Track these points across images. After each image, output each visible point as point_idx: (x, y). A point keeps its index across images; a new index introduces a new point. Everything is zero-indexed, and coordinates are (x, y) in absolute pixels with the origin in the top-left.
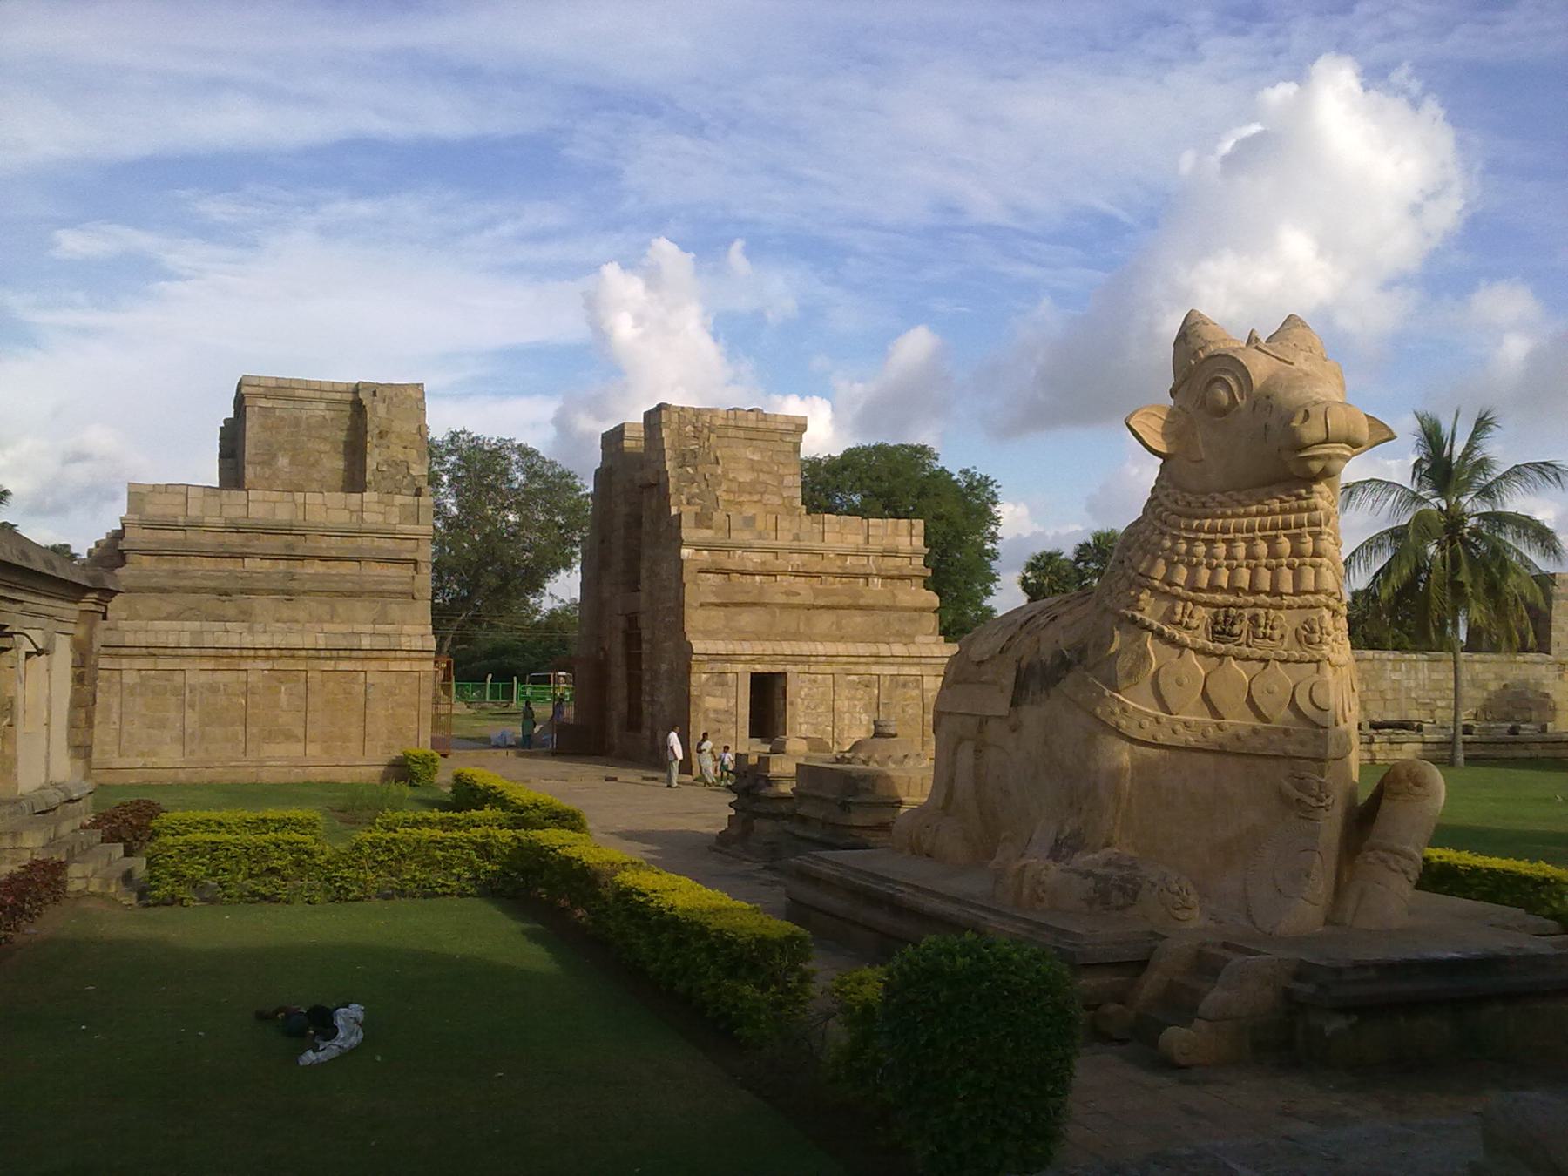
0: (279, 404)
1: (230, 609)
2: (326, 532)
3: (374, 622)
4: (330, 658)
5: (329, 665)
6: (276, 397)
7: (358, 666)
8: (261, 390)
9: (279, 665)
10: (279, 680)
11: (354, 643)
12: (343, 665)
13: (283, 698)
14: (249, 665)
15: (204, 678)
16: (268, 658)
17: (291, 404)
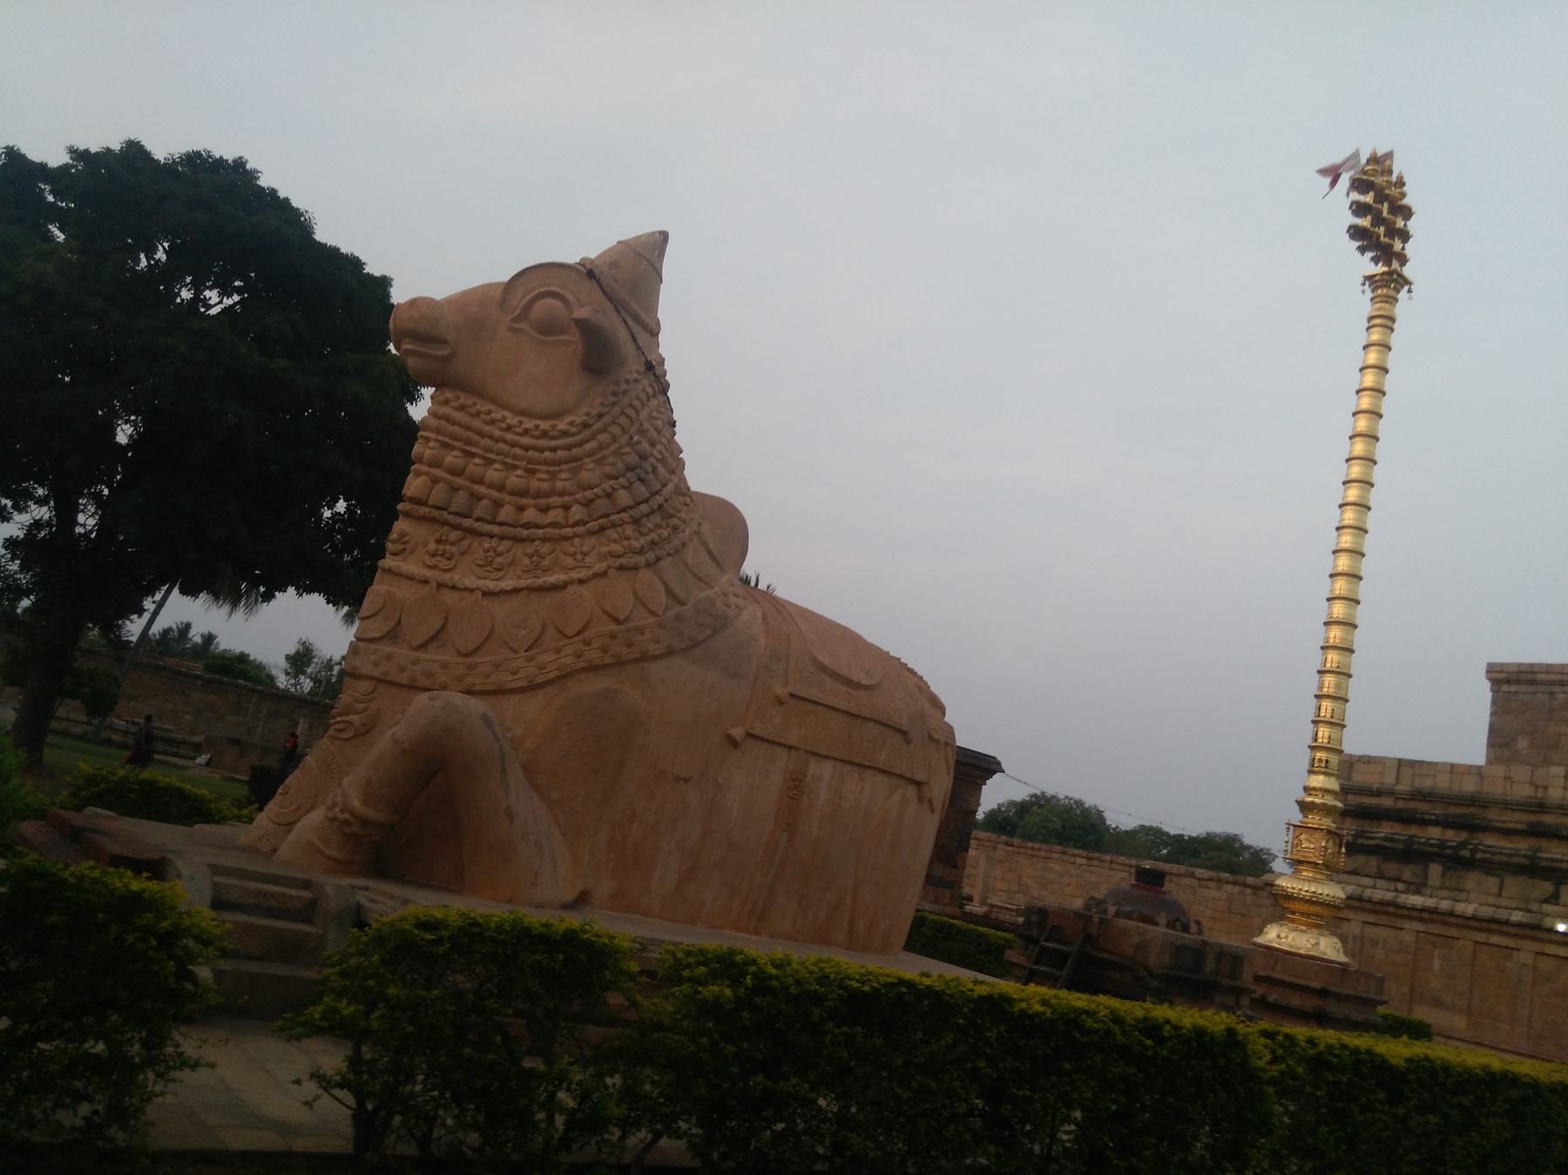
0: (1524, 688)
1: (1407, 873)
2: (1506, 805)
3: (1546, 901)
4: (1480, 930)
5: (1482, 937)
6: (1518, 682)
7: (1512, 943)
8: (1503, 676)
9: (1432, 928)
10: (1434, 944)
11: (1502, 914)
12: (1496, 939)
13: (1437, 964)
14: (1407, 924)
15: (1369, 931)
16: (1421, 920)
17: (1533, 688)
